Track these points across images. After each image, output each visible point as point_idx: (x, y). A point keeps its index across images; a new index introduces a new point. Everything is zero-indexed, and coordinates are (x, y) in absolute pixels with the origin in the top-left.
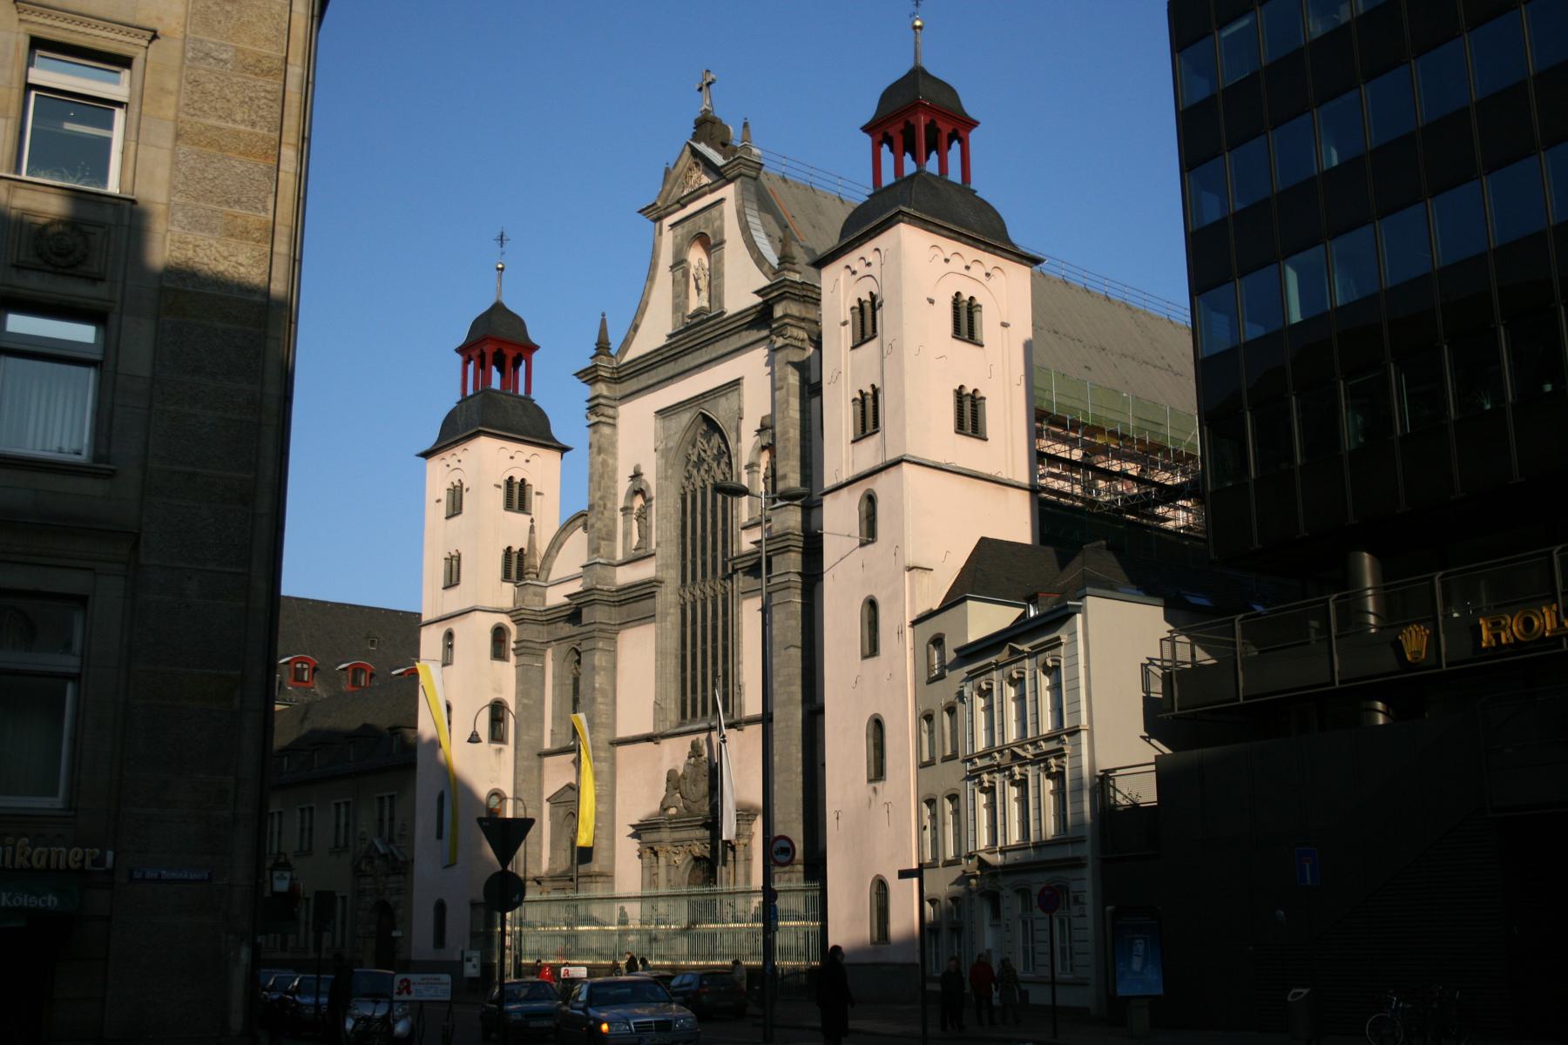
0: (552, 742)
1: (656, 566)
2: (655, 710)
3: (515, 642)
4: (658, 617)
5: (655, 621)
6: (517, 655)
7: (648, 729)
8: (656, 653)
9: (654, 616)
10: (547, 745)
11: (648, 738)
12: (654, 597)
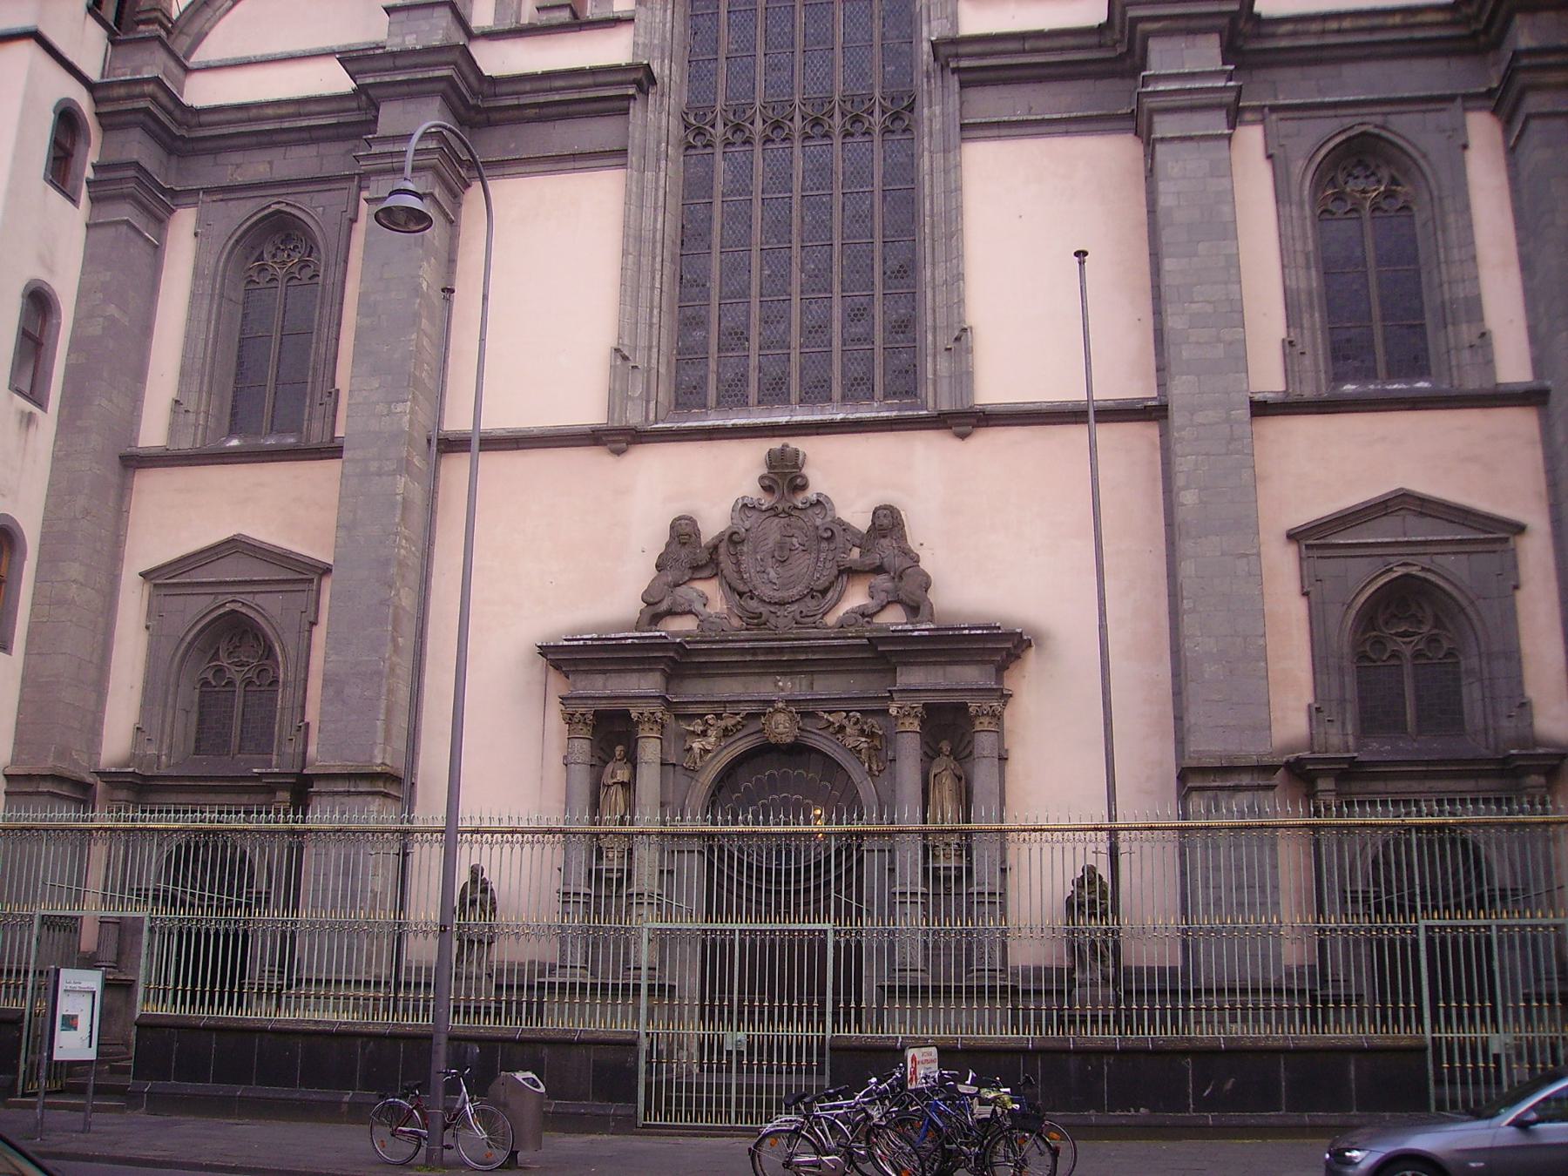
0: (173, 429)
1: (635, 44)
2: (613, 367)
3: (94, 166)
4: (633, 158)
5: (624, 166)
6: (94, 200)
7: (589, 412)
8: (626, 236)
9: (623, 152)
10: (153, 433)
11: (592, 438)
12: (626, 112)
